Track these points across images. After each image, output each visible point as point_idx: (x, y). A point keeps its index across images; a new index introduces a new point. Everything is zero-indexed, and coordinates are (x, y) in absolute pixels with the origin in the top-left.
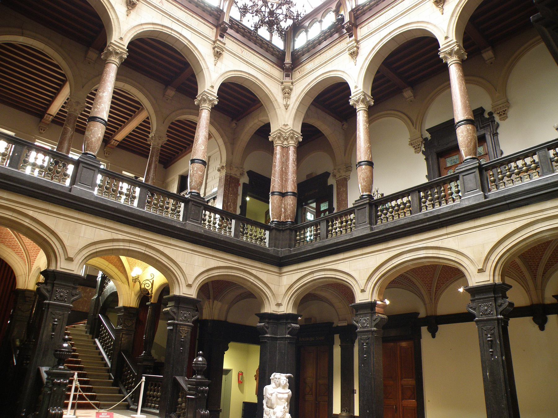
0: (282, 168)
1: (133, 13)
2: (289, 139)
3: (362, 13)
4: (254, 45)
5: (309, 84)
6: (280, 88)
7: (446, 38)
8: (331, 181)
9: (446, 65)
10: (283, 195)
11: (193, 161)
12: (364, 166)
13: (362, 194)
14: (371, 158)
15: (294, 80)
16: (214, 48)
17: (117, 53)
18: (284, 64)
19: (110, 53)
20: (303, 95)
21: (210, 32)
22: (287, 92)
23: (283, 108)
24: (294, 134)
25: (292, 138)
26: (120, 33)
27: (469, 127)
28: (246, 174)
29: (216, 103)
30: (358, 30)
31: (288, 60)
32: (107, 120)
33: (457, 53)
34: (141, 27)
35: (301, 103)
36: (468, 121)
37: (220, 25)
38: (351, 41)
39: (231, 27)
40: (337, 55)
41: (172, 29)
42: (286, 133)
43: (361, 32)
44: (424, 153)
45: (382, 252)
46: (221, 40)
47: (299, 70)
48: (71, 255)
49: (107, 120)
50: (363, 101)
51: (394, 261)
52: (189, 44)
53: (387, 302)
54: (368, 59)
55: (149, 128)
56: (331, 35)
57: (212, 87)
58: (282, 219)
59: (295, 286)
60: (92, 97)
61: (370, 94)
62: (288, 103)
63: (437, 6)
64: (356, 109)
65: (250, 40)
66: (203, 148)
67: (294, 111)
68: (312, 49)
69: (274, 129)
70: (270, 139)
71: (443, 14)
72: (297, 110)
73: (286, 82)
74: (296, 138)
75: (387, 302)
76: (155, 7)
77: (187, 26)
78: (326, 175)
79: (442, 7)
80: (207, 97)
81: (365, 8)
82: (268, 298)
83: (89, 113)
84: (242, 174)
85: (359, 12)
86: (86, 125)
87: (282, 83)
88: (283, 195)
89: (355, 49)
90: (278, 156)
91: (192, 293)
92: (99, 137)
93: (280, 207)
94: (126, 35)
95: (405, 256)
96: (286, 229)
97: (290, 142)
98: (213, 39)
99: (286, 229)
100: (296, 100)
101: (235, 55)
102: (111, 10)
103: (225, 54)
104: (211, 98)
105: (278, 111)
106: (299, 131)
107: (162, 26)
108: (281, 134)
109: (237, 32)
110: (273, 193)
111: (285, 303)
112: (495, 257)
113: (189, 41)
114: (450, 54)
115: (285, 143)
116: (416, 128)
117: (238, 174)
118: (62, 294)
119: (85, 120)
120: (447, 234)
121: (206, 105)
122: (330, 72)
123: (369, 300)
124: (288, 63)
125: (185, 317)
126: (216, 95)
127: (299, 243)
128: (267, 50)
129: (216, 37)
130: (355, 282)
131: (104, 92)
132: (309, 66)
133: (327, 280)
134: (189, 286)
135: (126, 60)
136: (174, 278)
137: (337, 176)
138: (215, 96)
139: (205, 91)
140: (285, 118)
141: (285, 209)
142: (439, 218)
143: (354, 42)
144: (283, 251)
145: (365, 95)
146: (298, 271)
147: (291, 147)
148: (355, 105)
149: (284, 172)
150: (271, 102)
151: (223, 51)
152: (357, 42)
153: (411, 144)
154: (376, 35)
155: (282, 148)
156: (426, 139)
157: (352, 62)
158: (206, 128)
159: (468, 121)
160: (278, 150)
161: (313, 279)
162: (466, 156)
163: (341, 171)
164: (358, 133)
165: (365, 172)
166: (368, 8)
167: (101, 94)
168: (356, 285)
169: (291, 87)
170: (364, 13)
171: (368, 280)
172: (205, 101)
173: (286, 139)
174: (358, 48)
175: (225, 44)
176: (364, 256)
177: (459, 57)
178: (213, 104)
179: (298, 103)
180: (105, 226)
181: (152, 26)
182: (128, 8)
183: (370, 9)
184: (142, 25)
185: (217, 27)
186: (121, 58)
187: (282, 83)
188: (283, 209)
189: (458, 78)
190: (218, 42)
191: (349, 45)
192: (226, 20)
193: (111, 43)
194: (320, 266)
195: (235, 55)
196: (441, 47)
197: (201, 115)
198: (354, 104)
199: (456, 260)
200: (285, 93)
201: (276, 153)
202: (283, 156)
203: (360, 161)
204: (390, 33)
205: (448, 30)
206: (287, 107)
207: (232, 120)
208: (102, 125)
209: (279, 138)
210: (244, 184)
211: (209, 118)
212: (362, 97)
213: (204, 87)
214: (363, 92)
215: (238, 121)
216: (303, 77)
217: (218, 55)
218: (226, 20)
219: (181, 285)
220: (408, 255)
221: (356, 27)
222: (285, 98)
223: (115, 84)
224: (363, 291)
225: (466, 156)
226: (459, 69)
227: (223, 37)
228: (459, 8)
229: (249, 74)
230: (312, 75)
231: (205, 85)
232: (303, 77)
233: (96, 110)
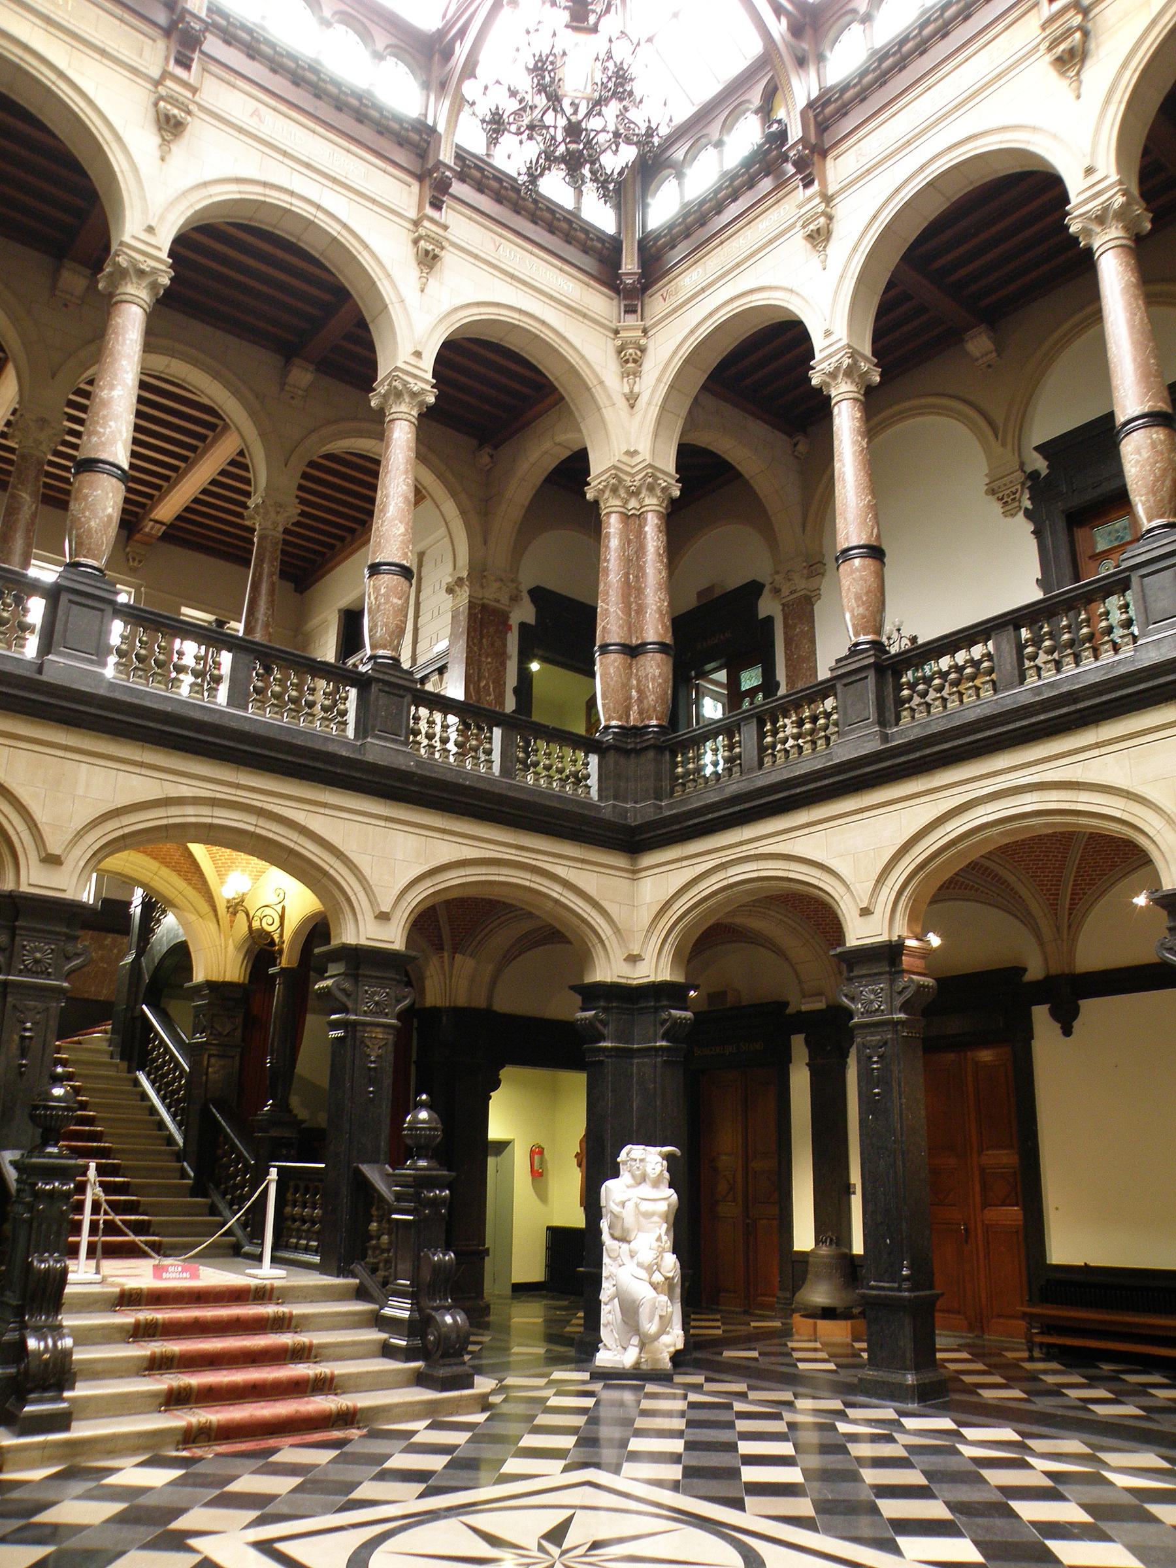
0: (627, 574)
1: (178, 149)
2: (644, 493)
3: (838, 111)
4: (531, 225)
5: (692, 332)
6: (611, 346)
7: (1089, 171)
8: (767, 606)
9: (1089, 253)
10: (633, 651)
11: (375, 569)
12: (857, 562)
13: (854, 640)
14: (878, 537)
15: (649, 323)
16: (416, 242)
17: (141, 273)
18: (618, 277)
19: (122, 274)
20: (677, 363)
21: (403, 195)
22: (631, 359)
23: (622, 404)
24: (656, 478)
25: (651, 488)
26: (145, 212)
27: (1158, 434)
28: (526, 599)
29: (431, 400)
31: (630, 265)
32: (126, 467)
33: (1122, 214)
34: (205, 192)
35: (671, 387)
36: (1154, 418)
37: (430, 173)
38: (810, 199)
39: (462, 177)
40: (771, 242)
41: (292, 193)
42: (633, 475)
43: (838, 169)
44: (1028, 514)
45: (917, 801)
46: (435, 214)
48: (54, 848)
49: (126, 467)
50: (849, 372)
51: (949, 826)
52: (344, 232)
53: (935, 940)
54: (861, 249)
55: (247, 481)
56: (751, 184)
57: (418, 354)
59: (675, 907)
60: (83, 403)
61: (867, 350)
62: (636, 389)
64: (829, 398)
65: (518, 213)
66: (402, 530)
67: (654, 411)
68: (698, 227)
69: (599, 465)
70: (590, 496)
72: (663, 408)
73: (627, 329)
74: (664, 490)
75: (935, 940)
76: (240, 130)
77: (335, 180)
78: (754, 589)
80: (405, 383)
81: (849, 95)
82: (602, 941)
83: (75, 447)
84: (515, 599)
85: (829, 110)
86: (67, 481)
87: (616, 332)
88: (633, 651)
89: (822, 220)
90: (614, 543)
91: (392, 936)
92: (110, 517)
93: (626, 686)
94: (162, 218)
95: (980, 810)
96: (646, 748)
97: (647, 502)
98: (413, 214)
99: (646, 748)
100: (659, 380)
101: (476, 257)
102: (115, 146)
103: (449, 258)
104: (416, 386)
105: (608, 413)
106: (671, 468)
107: (265, 184)
108: (620, 480)
109: (480, 188)
110: (604, 649)
111: (650, 952)
113: (345, 226)
114: (1101, 219)
115: (633, 503)
116: (1004, 445)
117: (505, 600)
118: (38, 955)
119: (67, 469)
120: (1098, 745)
121: (404, 408)
122: (751, 292)
123: (885, 938)
124: (631, 272)
125: (377, 1003)
126: (429, 376)
127: (683, 785)
128: (568, 239)
129: (420, 207)
130: (841, 889)
131: (112, 387)
132: (689, 279)
133: (765, 884)
134: (383, 917)
135: (168, 290)
136: (341, 899)
137: (785, 591)
138: (427, 381)
139: (396, 369)
140: (630, 434)
141: (639, 691)
142: (1075, 702)
143: (818, 200)
144: (638, 811)
145: (854, 354)
146: (685, 863)
147: (650, 516)
148: (828, 385)
149: (633, 586)
150: (588, 389)
151: (442, 248)
152: (827, 199)
153: (992, 492)
154: (882, 177)
155: (626, 518)
156: (1034, 476)
157: (815, 260)
158: (406, 472)
159: (1154, 418)
160: (613, 526)
161: (725, 883)
162: (1150, 521)
164: (837, 465)
165: (861, 578)
166: (857, 95)
167: (104, 394)
168: (847, 897)
169: (643, 342)
170: (843, 112)
171: (878, 881)
172: (399, 395)
173: (636, 494)
174: (830, 218)
175: (446, 228)
176: (866, 815)
177: (1126, 229)
178: (421, 404)
179: (663, 389)
180: (142, 765)
181: (234, 187)
182: (164, 139)
183: (862, 97)
184: (205, 184)
185: (420, 178)
186: (154, 286)
187: (616, 332)
188: (634, 693)
189: (1125, 290)
190: (426, 223)
191: (803, 211)
192: (446, 156)
193: (122, 244)
194: (745, 848)
195: (476, 257)
196: (1074, 200)
197: (390, 438)
198: (824, 383)
199: (1126, 817)
200: (627, 361)
202: (629, 542)
203: (846, 546)
204: (922, 168)
205: (1095, 145)
206: (632, 400)
207: (481, 446)
208: (114, 480)
209: (614, 490)
210: (523, 626)
211: (413, 445)
212: (847, 361)
213: (395, 356)
214: (849, 346)
215: (496, 447)
216: (675, 311)
217: (428, 260)
218: (446, 156)
219: (360, 917)
220: (990, 807)
221: (824, 154)
222: (625, 374)
223: (143, 361)
224: (865, 912)
225: (1150, 521)
226: (1128, 264)
227: (439, 208)
229: (520, 311)
230: (699, 305)
231: (395, 349)
232: (675, 311)
233: (94, 439)
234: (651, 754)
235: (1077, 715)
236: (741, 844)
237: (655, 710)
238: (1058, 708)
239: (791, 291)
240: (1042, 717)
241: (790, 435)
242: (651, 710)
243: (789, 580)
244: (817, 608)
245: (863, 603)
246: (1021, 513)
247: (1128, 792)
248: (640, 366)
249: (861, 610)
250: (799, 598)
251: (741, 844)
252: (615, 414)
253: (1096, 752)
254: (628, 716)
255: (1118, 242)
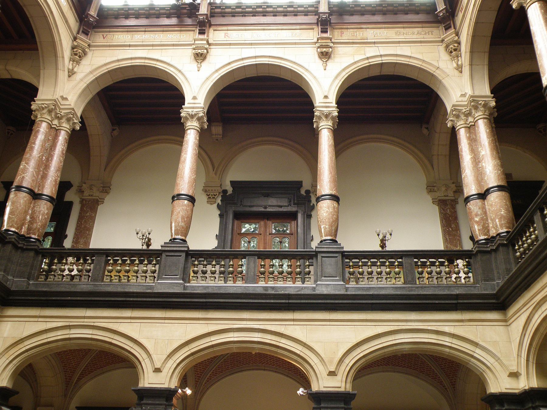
2: (64, 120)
5: (118, 61)
10: (35, 196)
13: (174, 237)
20: (104, 70)
25: (69, 120)
30: (211, 30)
35: (96, 79)
43: (215, 35)
44: (218, 206)
45: (198, 322)
47: (105, 34)
50: (199, 119)
51: (213, 338)
53: (189, 392)
54: (220, 72)
58: (23, 231)
59: (26, 343)
62: (75, 70)
63: (321, 58)
67: (83, 85)
70: (33, 107)
71: (325, 69)
74: (74, 123)
75: (189, 392)
79: (326, 61)
81: (227, 10)
89: (205, 51)
93: (26, 212)
95: (231, 334)
96: (31, 250)
97: (64, 125)
99: (31, 250)
100: (91, 72)
110: (19, 188)
112: (350, 361)
115: (56, 122)
116: (216, 174)
120: (294, 320)
123: (166, 386)
133: (93, 342)
137: (86, 193)
141: (32, 217)
142: (289, 299)
143: (205, 42)
146: (40, 319)
147: (63, 133)
153: (205, 191)
154: (234, 50)
155: (50, 127)
157: (195, 65)
160: (43, 128)
161: (67, 336)
163: (95, 189)
165: (186, 210)
168: (147, 360)
170: (223, 15)
171: (168, 356)
173: (59, 118)
176: (166, 321)
179: (92, 78)
187: (75, 39)
188: (28, 217)
189: (330, 146)
194: (86, 320)
199: (302, 354)
200: (76, 54)
201: (38, 131)
204: (256, 57)
205: (330, 89)
206: (71, 73)
209: (50, 112)
220: (236, 334)
221: (211, 25)
222: (72, 60)
224: (157, 370)
228: (344, 73)
234: (32, 254)
235: (287, 305)
236: (84, 317)
237: (39, 230)
238: (281, 299)
239: (180, 71)
240: (272, 301)
241: (113, 124)
242: (37, 230)
243: (91, 189)
244: (100, 207)
245: (185, 221)
246: (216, 205)
247: (305, 344)
248: (80, 60)
249: (183, 224)
250: (94, 199)
251: (84, 317)
252: (63, 75)
253: (292, 323)
254: (22, 228)
255: (329, 127)
